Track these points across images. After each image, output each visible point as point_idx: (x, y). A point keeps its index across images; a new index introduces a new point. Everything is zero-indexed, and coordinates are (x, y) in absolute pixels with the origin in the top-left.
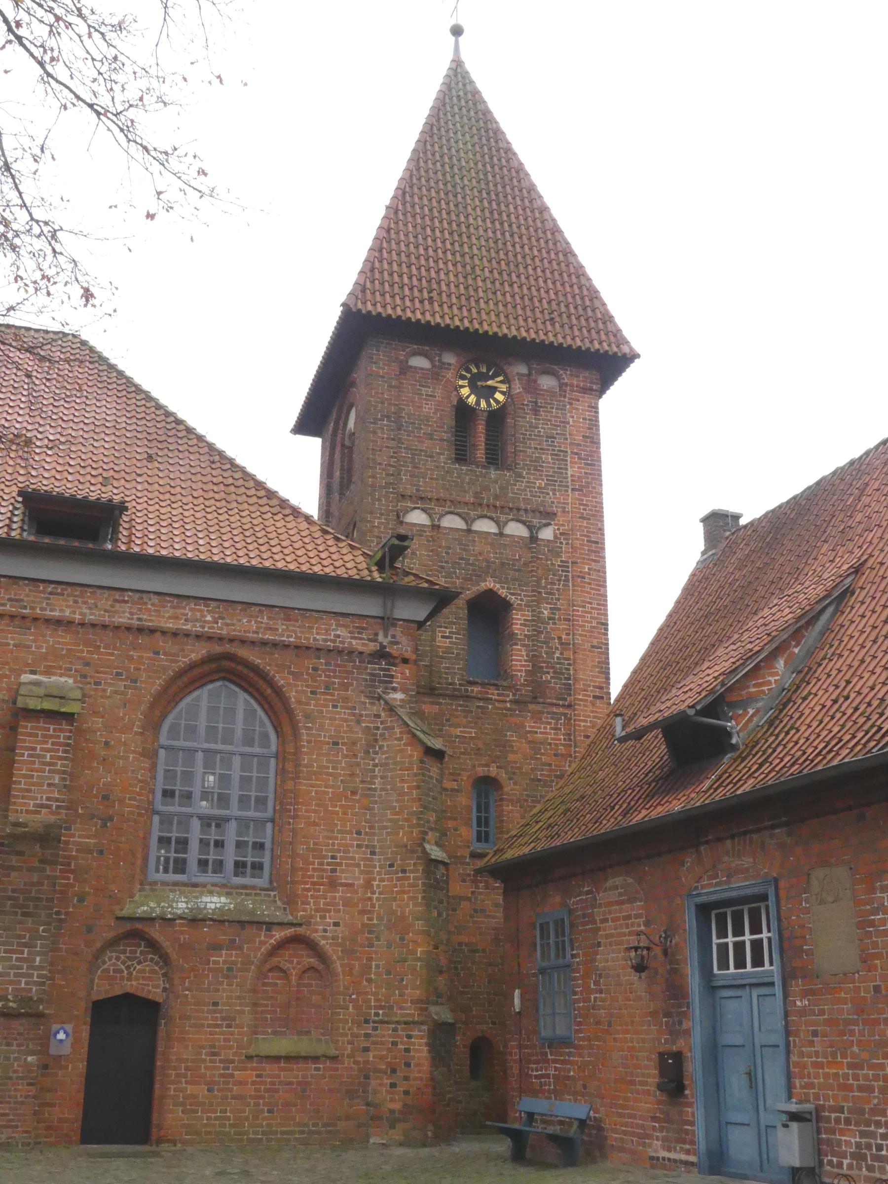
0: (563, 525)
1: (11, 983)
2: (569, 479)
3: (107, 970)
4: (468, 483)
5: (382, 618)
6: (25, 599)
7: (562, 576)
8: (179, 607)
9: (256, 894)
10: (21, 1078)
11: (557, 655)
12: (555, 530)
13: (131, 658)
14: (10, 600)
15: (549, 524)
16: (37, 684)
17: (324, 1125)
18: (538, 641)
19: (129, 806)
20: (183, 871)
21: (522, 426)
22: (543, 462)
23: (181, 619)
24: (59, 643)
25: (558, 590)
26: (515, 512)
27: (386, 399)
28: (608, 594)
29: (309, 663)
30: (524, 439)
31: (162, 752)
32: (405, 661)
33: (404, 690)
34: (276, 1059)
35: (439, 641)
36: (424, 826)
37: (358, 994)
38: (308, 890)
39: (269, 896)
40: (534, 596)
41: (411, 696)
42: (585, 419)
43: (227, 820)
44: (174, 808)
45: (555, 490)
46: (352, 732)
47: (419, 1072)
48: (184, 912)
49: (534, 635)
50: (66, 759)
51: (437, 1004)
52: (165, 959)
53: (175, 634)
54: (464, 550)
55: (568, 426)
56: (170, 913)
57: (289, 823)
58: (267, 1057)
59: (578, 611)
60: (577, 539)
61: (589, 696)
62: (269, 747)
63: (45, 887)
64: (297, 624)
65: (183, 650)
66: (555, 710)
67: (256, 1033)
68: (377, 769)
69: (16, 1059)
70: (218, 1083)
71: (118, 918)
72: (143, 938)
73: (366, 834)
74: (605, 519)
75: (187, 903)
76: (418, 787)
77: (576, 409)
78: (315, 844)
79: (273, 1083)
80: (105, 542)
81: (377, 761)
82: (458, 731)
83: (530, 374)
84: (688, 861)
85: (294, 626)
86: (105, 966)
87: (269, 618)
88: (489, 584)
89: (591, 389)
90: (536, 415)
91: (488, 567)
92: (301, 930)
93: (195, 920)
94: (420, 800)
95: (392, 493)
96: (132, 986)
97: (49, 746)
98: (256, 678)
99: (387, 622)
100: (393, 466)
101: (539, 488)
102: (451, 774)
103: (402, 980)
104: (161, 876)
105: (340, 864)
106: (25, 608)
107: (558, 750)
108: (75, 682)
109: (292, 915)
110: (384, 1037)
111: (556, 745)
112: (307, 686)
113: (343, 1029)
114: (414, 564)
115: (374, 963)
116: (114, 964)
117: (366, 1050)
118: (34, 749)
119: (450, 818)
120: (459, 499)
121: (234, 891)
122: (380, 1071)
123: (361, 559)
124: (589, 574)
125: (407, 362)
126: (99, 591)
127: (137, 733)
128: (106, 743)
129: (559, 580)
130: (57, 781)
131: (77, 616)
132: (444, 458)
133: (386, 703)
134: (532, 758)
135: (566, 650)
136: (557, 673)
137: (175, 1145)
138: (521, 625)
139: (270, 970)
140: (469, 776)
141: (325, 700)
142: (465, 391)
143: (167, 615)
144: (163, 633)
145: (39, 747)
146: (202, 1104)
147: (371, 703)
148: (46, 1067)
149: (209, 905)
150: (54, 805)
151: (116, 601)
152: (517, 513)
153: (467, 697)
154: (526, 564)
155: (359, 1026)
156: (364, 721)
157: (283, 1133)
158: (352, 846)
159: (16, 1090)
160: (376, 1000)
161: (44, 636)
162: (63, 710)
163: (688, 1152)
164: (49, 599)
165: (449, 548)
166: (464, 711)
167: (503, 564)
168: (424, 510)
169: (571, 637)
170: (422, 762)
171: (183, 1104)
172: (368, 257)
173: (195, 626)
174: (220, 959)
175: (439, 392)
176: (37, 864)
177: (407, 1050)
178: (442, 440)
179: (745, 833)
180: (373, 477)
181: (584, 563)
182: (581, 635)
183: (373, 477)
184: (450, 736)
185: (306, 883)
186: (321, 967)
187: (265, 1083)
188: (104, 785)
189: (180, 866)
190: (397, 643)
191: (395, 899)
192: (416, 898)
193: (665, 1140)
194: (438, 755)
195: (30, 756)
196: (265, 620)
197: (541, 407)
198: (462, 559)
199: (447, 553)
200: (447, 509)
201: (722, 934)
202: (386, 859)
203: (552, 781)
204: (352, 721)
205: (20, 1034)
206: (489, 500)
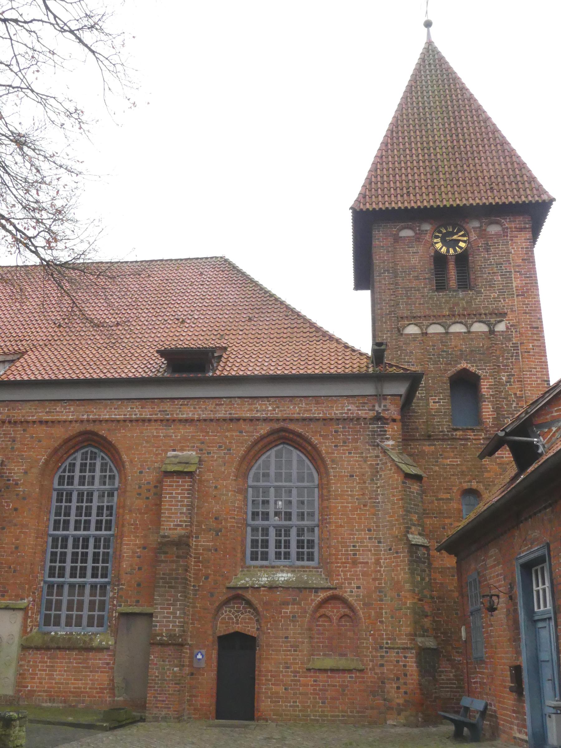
0: (512, 320)
1: (165, 626)
2: (514, 289)
3: (224, 618)
4: (444, 303)
5: (376, 395)
7: (514, 353)
8: (252, 404)
9: (310, 571)
11: (514, 405)
12: (506, 324)
13: (226, 437)
14: (160, 411)
15: (502, 321)
16: (176, 457)
17: (358, 712)
20: (266, 559)
21: (478, 261)
22: (495, 281)
25: (512, 362)
26: (478, 316)
27: (386, 260)
28: (548, 360)
29: (333, 428)
30: (481, 268)
31: (250, 490)
32: (394, 420)
33: (393, 439)
34: (325, 671)
35: (432, 406)
36: (407, 523)
38: (340, 567)
39: (318, 571)
40: (495, 369)
41: (399, 442)
43: (292, 527)
44: (259, 522)
45: (505, 298)
47: (412, 680)
48: (265, 584)
49: (497, 394)
50: (188, 498)
51: (423, 636)
53: (251, 420)
55: (511, 255)
56: (257, 584)
57: (327, 527)
58: (319, 670)
60: (523, 327)
62: (313, 482)
63: (180, 571)
64: (324, 406)
65: (256, 429)
67: (313, 655)
68: (379, 490)
69: (168, 669)
71: (228, 588)
72: (244, 600)
73: (374, 530)
74: (542, 311)
75: (267, 577)
76: (402, 499)
77: (515, 243)
79: (324, 686)
80: (208, 372)
81: (379, 485)
82: (448, 461)
83: (481, 226)
85: (322, 407)
87: (306, 404)
88: (464, 365)
89: (525, 228)
90: (487, 252)
91: (461, 354)
92: (336, 592)
93: (272, 588)
95: (394, 317)
96: (239, 627)
101: (494, 298)
102: (446, 489)
105: (359, 550)
106: (168, 414)
108: (196, 454)
109: (330, 582)
110: (392, 657)
112: (332, 443)
114: (412, 359)
115: (384, 611)
116: (227, 615)
117: (382, 665)
118: (172, 493)
119: (446, 518)
120: (439, 314)
121: (297, 570)
122: (389, 679)
123: (365, 360)
124: (533, 349)
126: (207, 401)
127: (232, 480)
128: (216, 487)
129: (512, 356)
130: (185, 511)
131: (196, 416)
133: (382, 448)
135: (520, 401)
137: (267, 721)
139: (321, 616)
140: (458, 489)
141: (343, 450)
142: (439, 246)
143: (246, 409)
144: (245, 420)
147: (372, 449)
149: (280, 579)
150: (184, 524)
152: (478, 317)
153: (454, 439)
154: (488, 349)
155: (376, 649)
156: (369, 461)
159: (169, 687)
160: (386, 635)
161: (179, 429)
162: (185, 470)
164: (180, 408)
165: (435, 346)
166: (451, 448)
168: (416, 325)
169: (523, 392)
170: (404, 483)
171: (270, 697)
172: (368, 176)
174: (288, 610)
177: (405, 666)
178: (425, 279)
179: (535, 514)
180: (381, 309)
181: (529, 343)
182: (529, 390)
183: (381, 309)
185: (338, 563)
186: (351, 614)
187: (319, 685)
188: (216, 511)
189: (265, 557)
190: (388, 410)
191: (393, 571)
194: (418, 478)
195: (169, 497)
197: (490, 246)
199: (433, 349)
200: (431, 322)
204: (361, 461)
205: (170, 655)
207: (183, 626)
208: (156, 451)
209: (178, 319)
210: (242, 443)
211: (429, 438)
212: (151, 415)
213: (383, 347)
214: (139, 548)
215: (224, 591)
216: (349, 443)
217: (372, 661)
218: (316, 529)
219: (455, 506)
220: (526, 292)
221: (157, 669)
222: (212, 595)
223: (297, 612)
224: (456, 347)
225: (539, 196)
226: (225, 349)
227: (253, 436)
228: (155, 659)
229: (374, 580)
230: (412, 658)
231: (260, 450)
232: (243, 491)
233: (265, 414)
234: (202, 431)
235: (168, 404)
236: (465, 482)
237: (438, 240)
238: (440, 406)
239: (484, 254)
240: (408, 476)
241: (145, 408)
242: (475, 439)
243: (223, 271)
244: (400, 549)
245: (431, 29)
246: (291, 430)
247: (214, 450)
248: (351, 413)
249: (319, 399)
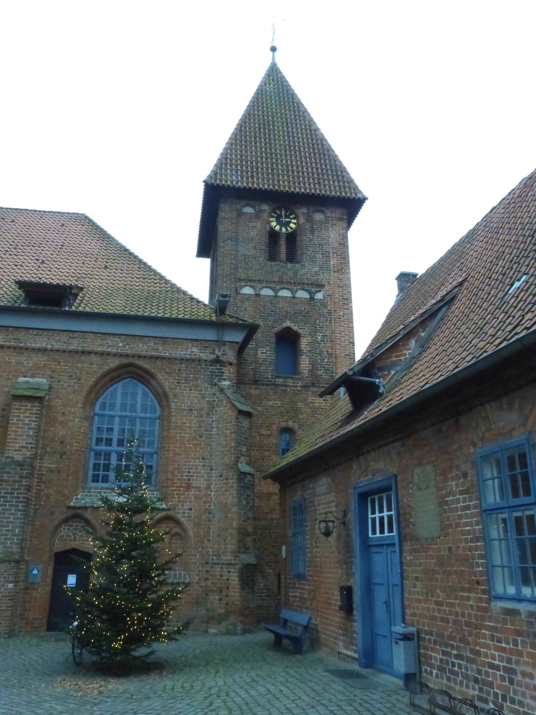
0: (328, 291)
2: (332, 267)
4: (276, 271)
5: (217, 341)
6: (22, 338)
7: (328, 318)
11: (326, 360)
12: (324, 294)
13: (77, 368)
14: (14, 339)
16: (27, 382)
18: (315, 353)
19: (75, 446)
22: (317, 258)
24: (39, 361)
25: (326, 325)
26: (302, 285)
29: (176, 367)
31: (96, 418)
32: (231, 364)
35: (260, 356)
38: (175, 490)
40: (313, 329)
42: (340, 234)
44: (103, 447)
46: (200, 404)
54: (274, 307)
59: (337, 336)
60: (336, 298)
68: (214, 423)
71: (69, 507)
73: (208, 459)
74: (352, 287)
76: (234, 432)
78: (178, 465)
80: (65, 307)
81: (214, 419)
82: (270, 403)
83: (309, 213)
84: (354, 466)
87: (154, 344)
88: (288, 324)
89: (344, 219)
90: (313, 234)
92: (169, 513)
94: (235, 439)
97: (27, 415)
99: (220, 343)
100: (233, 264)
103: (226, 540)
104: (95, 484)
105: (193, 476)
106: (22, 343)
110: (216, 572)
112: (175, 379)
114: (246, 315)
117: (207, 579)
118: (20, 417)
119: (266, 450)
120: (270, 280)
122: (212, 591)
125: (241, 210)
127: (80, 407)
128: (63, 413)
129: (327, 320)
130: (31, 434)
132: (262, 258)
133: (219, 387)
134: (312, 417)
135: (331, 357)
136: (326, 370)
141: (185, 387)
142: (274, 224)
143: (98, 344)
145: (22, 415)
147: (210, 388)
148: (26, 589)
150: (30, 446)
151: (70, 337)
152: (303, 286)
153: (275, 385)
154: (308, 312)
155: (203, 566)
158: (199, 466)
160: (212, 552)
161: (31, 357)
162: (36, 395)
163: (355, 652)
164: (34, 338)
165: (265, 306)
167: (295, 313)
168: (251, 286)
169: (333, 350)
170: (237, 418)
173: (113, 349)
175: (259, 225)
177: (228, 580)
180: (223, 270)
182: (339, 349)
184: (267, 406)
185: (173, 487)
186: (182, 533)
191: (223, 495)
192: (233, 494)
193: (344, 642)
194: (248, 415)
198: (272, 311)
199: (264, 309)
201: (373, 512)
202: (218, 473)
204: (199, 397)
206: (287, 279)
207: (21, 544)
208: (7, 376)
209: (38, 260)
211: (256, 382)
212: (4, 342)
213: (227, 299)
215: (65, 510)
216: (190, 380)
217: (197, 575)
218: (155, 456)
219: (274, 441)
220: (340, 270)
222: (52, 513)
224: (282, 308)
225: (356, 194)
226: (82, 289)
227: (104, 368)
229: (205, 502)
230: (235, 572)
231: (109, 382)
232: (89, 419)
234: (54, 361)
235: (23, 333)
236: (283, 421)
237: (274, 219)
238: (266, 356)
239: (309, 236)
240: (241, 412)
242: (294, 386)
243: (83, 226)
244: (229, 476)
245: (275, 53)
248: (194, 355)
249: (166, 340)
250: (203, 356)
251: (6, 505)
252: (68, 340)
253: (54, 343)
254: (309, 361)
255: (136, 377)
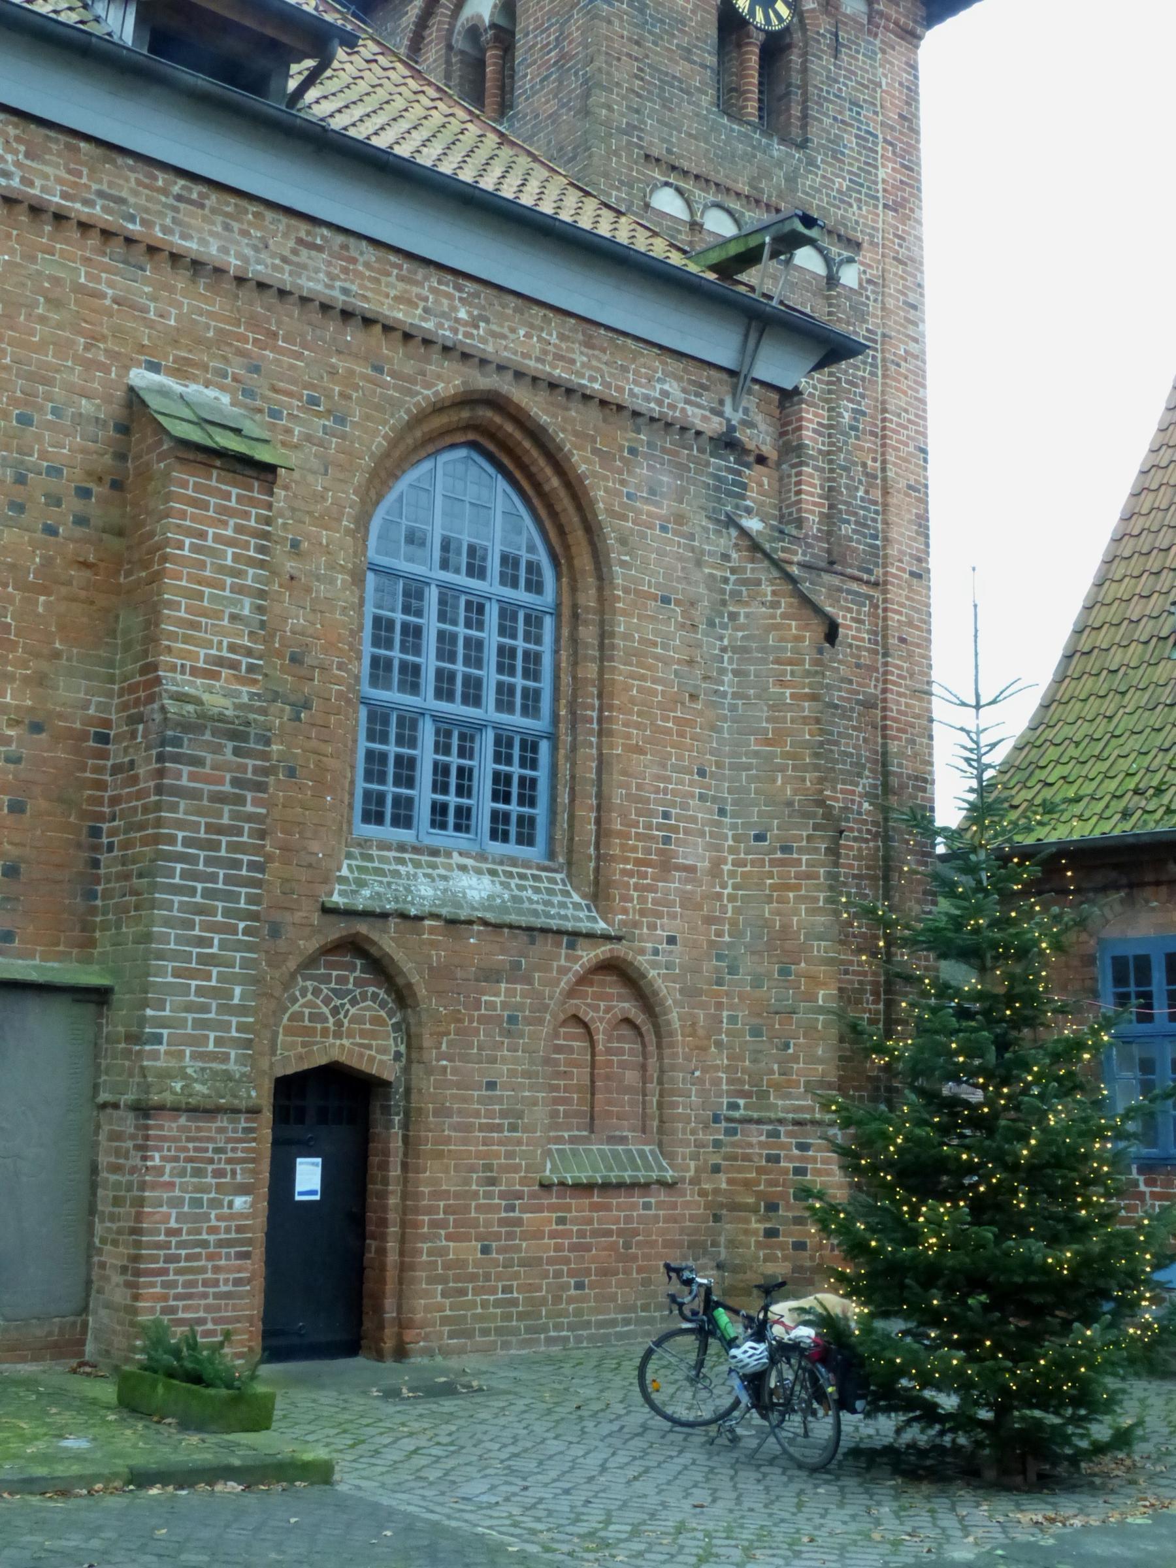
2: (880, 187)
5: (732, 373)
6: (132, 200)
10: (229, 1243)
13: (333, 372)
14: (101, 194)
21: (817, 73)
23: (416, 306)
32: (761, 460)
37: (704, 1071)
38: (630, 874)
43: (481, 728)
44: (393, 696)
45: (859, 200)
52: (402, 997)
61: (904, 570)
66: (855, 586)
70: (497, 1237)
71: (328, 911)
78: (639, 787)
85: (599, 360)
86: (296, 1007)
87: (561, 337)
90: (836, 57)
92: (620, 949)
94: (818, 721)
97: (229, 532)
98: (535, 453)
103: (787, 1046)
104: (371, 831)
105: (675, 829)
106: (132, 219)
107: (859, 657)
108: (232, 404)
109: (605, 920)
111: (858, 647)
113: (684, 1133)
115: (725, 1014)
117: (716, 1169)
120: (729, 183)
126: (269, 215)
127: (348, 532)
128: (295, 544)
130: (246, 612)
132: (706, 100)
138: (814, 431)
143: (393, 293)
144: (387, 329)
145: (211, 531)
146: (473, 1278)
150: (245, 661)
151: (300, 241)
155: (706, 1127)
157: (601, 1324)
159: (216, 1269)
160: (730, 1082)
164: (176, 210)
168: (679, 191)
171: (443, 1280)
173: (441, 326)
174: (497, 997)
176: (227, 788)
180: (610, 108)
182: (895, 464)
183: (610, 108)
185: (626, 860)
186: (640, 1019)
196: (554, 339)
203: (852, 710)
205: (217, 1150)
206: (770, 197)
208: (87, 347)
210: (378, 408)
212: (65, 195)
214: (14, 723)
215: (316, 918)
216: (662, 495)
217: (695, 1157)
221: (176, 1203)
223: (520, 1007)
228: (168, 1167)
233: (451, 329)
234: (254, 323)
241: (45, 163)
246: (518, 407)
247: (291, 407)
249: (592, 331)
250: (696, 416)
251: (192, 892)
252: (295, 252)
253: (248, 252)
254: (822, 488)
255: (491, 447)
